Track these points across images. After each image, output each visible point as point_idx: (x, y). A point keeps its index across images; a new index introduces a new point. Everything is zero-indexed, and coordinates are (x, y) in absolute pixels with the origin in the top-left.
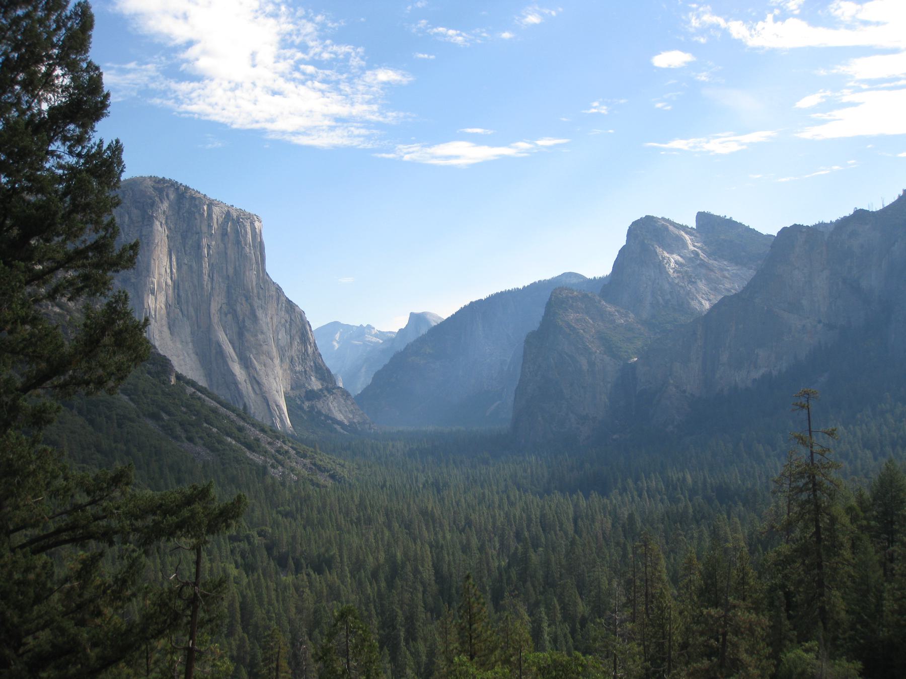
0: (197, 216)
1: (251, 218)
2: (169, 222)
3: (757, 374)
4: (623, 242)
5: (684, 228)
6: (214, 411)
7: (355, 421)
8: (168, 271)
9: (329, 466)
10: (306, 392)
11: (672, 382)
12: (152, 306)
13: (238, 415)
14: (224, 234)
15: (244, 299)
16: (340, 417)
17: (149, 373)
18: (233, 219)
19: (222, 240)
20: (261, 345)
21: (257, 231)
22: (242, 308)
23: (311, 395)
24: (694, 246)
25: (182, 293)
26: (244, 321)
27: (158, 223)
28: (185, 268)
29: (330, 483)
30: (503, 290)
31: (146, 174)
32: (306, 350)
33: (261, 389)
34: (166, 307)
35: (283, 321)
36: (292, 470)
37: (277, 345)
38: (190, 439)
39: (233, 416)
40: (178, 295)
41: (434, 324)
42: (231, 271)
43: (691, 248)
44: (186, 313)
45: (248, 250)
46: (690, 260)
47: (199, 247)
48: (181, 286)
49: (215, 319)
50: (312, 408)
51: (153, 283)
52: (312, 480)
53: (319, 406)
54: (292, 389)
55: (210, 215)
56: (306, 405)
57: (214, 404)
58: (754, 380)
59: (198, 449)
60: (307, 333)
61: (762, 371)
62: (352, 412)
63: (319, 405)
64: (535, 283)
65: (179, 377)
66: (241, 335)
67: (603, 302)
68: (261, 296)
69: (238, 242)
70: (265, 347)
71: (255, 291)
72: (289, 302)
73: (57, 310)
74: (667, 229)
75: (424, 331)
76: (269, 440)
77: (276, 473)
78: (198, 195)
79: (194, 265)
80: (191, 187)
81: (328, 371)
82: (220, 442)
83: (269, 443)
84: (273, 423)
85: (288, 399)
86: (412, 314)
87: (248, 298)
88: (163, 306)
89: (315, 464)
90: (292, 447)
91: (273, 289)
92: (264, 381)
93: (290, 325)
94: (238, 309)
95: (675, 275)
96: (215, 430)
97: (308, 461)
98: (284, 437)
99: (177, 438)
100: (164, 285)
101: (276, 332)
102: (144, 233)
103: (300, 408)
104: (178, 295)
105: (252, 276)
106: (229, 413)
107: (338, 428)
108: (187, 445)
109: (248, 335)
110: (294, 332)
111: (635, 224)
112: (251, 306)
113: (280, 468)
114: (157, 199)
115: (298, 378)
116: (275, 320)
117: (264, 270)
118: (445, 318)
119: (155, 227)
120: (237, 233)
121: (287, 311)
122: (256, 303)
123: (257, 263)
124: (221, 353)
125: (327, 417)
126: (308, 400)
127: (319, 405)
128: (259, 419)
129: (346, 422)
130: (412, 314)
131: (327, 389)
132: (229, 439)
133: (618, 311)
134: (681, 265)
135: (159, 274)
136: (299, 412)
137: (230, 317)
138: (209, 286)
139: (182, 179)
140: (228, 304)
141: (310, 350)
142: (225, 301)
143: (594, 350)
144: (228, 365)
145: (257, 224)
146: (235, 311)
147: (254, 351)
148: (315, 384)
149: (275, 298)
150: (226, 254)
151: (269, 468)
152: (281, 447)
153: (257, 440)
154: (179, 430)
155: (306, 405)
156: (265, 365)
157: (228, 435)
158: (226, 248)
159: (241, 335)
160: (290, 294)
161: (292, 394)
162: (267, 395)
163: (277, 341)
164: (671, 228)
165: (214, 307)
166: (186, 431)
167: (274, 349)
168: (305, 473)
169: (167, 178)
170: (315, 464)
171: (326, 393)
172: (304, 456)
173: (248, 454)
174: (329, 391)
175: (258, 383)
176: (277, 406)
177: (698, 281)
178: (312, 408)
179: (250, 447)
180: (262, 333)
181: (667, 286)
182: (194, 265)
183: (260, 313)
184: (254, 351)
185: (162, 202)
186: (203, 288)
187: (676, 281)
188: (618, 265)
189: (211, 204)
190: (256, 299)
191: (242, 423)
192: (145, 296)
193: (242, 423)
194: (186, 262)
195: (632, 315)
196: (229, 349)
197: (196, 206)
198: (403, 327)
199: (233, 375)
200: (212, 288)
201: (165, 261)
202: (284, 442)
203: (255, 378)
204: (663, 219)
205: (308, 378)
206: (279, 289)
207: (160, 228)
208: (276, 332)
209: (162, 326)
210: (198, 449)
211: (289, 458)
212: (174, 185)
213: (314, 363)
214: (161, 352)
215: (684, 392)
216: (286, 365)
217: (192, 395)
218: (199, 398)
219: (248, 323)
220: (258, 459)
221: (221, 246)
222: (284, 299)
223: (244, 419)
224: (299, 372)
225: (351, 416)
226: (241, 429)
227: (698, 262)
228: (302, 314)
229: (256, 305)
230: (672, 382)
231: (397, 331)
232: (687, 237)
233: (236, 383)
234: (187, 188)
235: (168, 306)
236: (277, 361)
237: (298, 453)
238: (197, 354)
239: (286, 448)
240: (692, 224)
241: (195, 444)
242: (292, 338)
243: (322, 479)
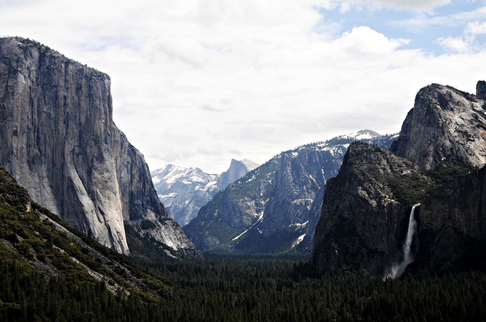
0: (56, 71)
1: (103, 77)
2: (32, 76)
4: (413, 106)
5: (465, 95)
6: (63, 235)
7: (182, 247)
8: (30, 117)
9: (158, 284)
10: (142, 222)
11: (451, 224)
12: (15, 146)
13: (84, 240)
14: (79, 88)
15: (93, 143)
16: (170, 244)
17: (8, 201)
18: (86, 76)
19: (77, 93)
20: (106, 181)
21: (106, 86)
22: (92, 150)
23: (148, 225)
24: (474, 110)
25: (42, 137)
26: (92, 161)
27: (22, 77)
28: (44, 115)
29: (157, 299)
30: (309, 143)
31: (14, 35)
32: (144, 187)
33: (104, 219)
34: (27, 148)
35: (126, 163)
36: (126, 286)
37: (120, 182)
38: (41, 259)
39: (79, 240)
40: (38, 138)
41: (251, 169)
42: (83, 119)
43: (472, 111)
44: (43, 152)
45: (98, 102)
46: (471, 122)
47: (57, 97)
48: (40, 131)
49: (68, 159)
50: (147, 235)
51: (16, 126)
52: (142, 296)
53: (152, 234)
54: (131, 219)
55: (66, 72)
56: (142, 233)
57: (64, 229)
59: (47, 267)
60: (146, 173)
62: (179, 239)
63: (153, 233)
64: (336, 138)
65: (34, 206)
67: (393, 156)
68: (108, 142)
69: (90, 96)
70: (110, 184)
71: (103, 137)
72: (131, 146)
74: (451, 96)
75: (242, 174)
76: (109, 261)
77: (112, 289)
78: (56, 55)
79: (52, 112)
80: (52, 48)
81: (162, 205)
82: (66, 261)
83: (108, 264)
84: (113, 246)
85: (127, 227)
87: (97, 142)
88: (24, 146)
89: (146, 283)
90: (129, 269)
91: (118, 135)
92: (108, 211)
93: (132, 167)
94: (88, 151)
95: (456, 134)
97: (140, 280)
98: (121, 259)
99: (30, 257)
100: (26, 130)
102: (10, 84)
103: (138, 235)
104: (38, 138)
105: (100, 126)
106: (76, 237)
107: (168, 253)
108: (38, 263)
109: (96, 174)
110: (134, 171)
111: (423, 90)
112: (99, 148)
113: (116, 285)
114: (22, 56)
115: (136, 210)
116: (119, 161)
117: (111, 119)
118: (260, 165)
119: (19, 80)
120: (90, 88)
121: (129, 154)
122: (104, 146)
123: (105, 113)
125: (159, 243)
126: (144, 229)
127: (153, 233)
128: (102, 244)
129: (175, 248)
131: (160, 220)
132: (74, 259)
133: (406, 164)
134: (462, 125)
135: (22, 119)
136: (136, 239)
137: (80, 157)
138: (65, 131)
139: (45, 42)
140: (80, 146)
141: (148, 187)
142: (77, 144)
143: (383, 195)
144: (78, 198)
145: (106, 81)
146: (86, 153)
147: (100, 186)
148: (151, 216)
149: (119, 143)
150: (80, 105)
151: (107, 285)
152: (118, 267)
153: (98, 260)
154: (31, 250)
155: (143, 232)
156: (109, 198)
158: (79, 100)
159: (89, 173)
160: (132, 139)
161: (130, 223)
162: (109, 223)
163: (120, 179)
164: (454, 94)
165: (68, 149)
166: (37, 251)
167: (117, 186)
168: (138, 290)
169: (31, 39)
170: (146, 283)
171: (159, 223)
172: (139, 276)
174: (162, 222)
175: (103, 213)
176: (118, 232)
177: (476, 139)
178: (147, 235)
180: (108, 171)
181: (448, 143)
182: (52, 112)
183: (106, 155)
184: (100, 186)
185: (26, 59)
186: (59, 132)
187: (457, 139)
188: (406, 126)
189: (68, 62)
190: (103, 143)
192: (9, 137)
193: (86, 246)
194: (45, 110)
195: (416, 167)
196: (78, 183)
197: (55, 63)
198: (226, 170)
199: (81, 205)
200: (67, 133)
201: (28, 109)
202: (121, 263)
203: (99, 209)
204: (448, 87)
205: (145, 211)
206: (123, 136)
207: (24, 81)
208: (119, 171)
209: (22, 163)
210: (47, 267)
211: (125, 277)
212: (36, 45)
213: (150, 198)
214: (21, 185)
215: (462, 233)
216: (127, 200)
217: (45, 222)
219: (96, 164)
220: (97, 276)
221: (76, 98)
222: (127, 144)
223: (88, 243)
224: (137, 205)
225: (179, 243)
227: (477, 123)
228: (141, 158)
229: (103, 148)
230: (451, 224)
231: (220, 173)
232: (467, 102)
233: (83, 213)
234: (47, 49)
235: (29, 146)
236: (118, 195)
237: (133, 273)
238: (52, 188)
239: (122, 268)
240: (473, 90)
241: (45, 262)
242: (132, 177)
243: (150, 295)
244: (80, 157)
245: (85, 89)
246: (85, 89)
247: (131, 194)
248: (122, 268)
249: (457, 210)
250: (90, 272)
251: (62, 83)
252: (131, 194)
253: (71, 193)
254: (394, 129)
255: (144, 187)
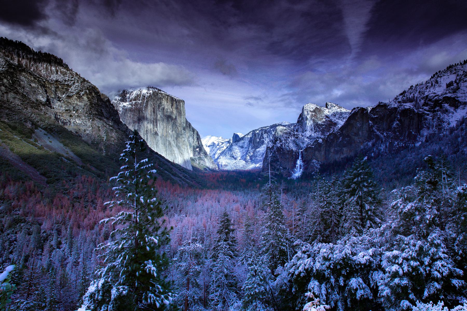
3: (342, 156)
6: (163, 163)
14: (172, 106)
19: (172, 108)
36: (187, 182)
54: (194, 156)
55: (167, 99)
58: (342, 158)
61: (345, 155)
66: (177, 138)
73: (111, 128)
82: (162, 172)
86: (234, 134)
96: (162, 169)
101: (189, 138)
124: (170, 144)
130: (234, 134)
132: (166, 172)
147: (181, 144)
157: (166, 170)
173: (172, 177)
179: (173, 175)
189: (168, 96)
191: (172, 167)
196: (172, 143)
218: (158, 159)
226: (171, 169)
228: (197, 133)
239: (186, 175)
244: (173, 132)
245: (175, 105)
246: (175, 105)
247: (194, 146)
248: (186, 175)
249: (317, 152)
250: (172, 177)
251: (166, 103)
252: (194, 146)
253: (170, 147)
254: (295, 121)
255: (199, 143)
